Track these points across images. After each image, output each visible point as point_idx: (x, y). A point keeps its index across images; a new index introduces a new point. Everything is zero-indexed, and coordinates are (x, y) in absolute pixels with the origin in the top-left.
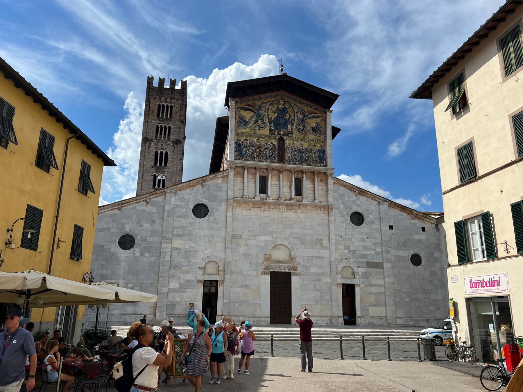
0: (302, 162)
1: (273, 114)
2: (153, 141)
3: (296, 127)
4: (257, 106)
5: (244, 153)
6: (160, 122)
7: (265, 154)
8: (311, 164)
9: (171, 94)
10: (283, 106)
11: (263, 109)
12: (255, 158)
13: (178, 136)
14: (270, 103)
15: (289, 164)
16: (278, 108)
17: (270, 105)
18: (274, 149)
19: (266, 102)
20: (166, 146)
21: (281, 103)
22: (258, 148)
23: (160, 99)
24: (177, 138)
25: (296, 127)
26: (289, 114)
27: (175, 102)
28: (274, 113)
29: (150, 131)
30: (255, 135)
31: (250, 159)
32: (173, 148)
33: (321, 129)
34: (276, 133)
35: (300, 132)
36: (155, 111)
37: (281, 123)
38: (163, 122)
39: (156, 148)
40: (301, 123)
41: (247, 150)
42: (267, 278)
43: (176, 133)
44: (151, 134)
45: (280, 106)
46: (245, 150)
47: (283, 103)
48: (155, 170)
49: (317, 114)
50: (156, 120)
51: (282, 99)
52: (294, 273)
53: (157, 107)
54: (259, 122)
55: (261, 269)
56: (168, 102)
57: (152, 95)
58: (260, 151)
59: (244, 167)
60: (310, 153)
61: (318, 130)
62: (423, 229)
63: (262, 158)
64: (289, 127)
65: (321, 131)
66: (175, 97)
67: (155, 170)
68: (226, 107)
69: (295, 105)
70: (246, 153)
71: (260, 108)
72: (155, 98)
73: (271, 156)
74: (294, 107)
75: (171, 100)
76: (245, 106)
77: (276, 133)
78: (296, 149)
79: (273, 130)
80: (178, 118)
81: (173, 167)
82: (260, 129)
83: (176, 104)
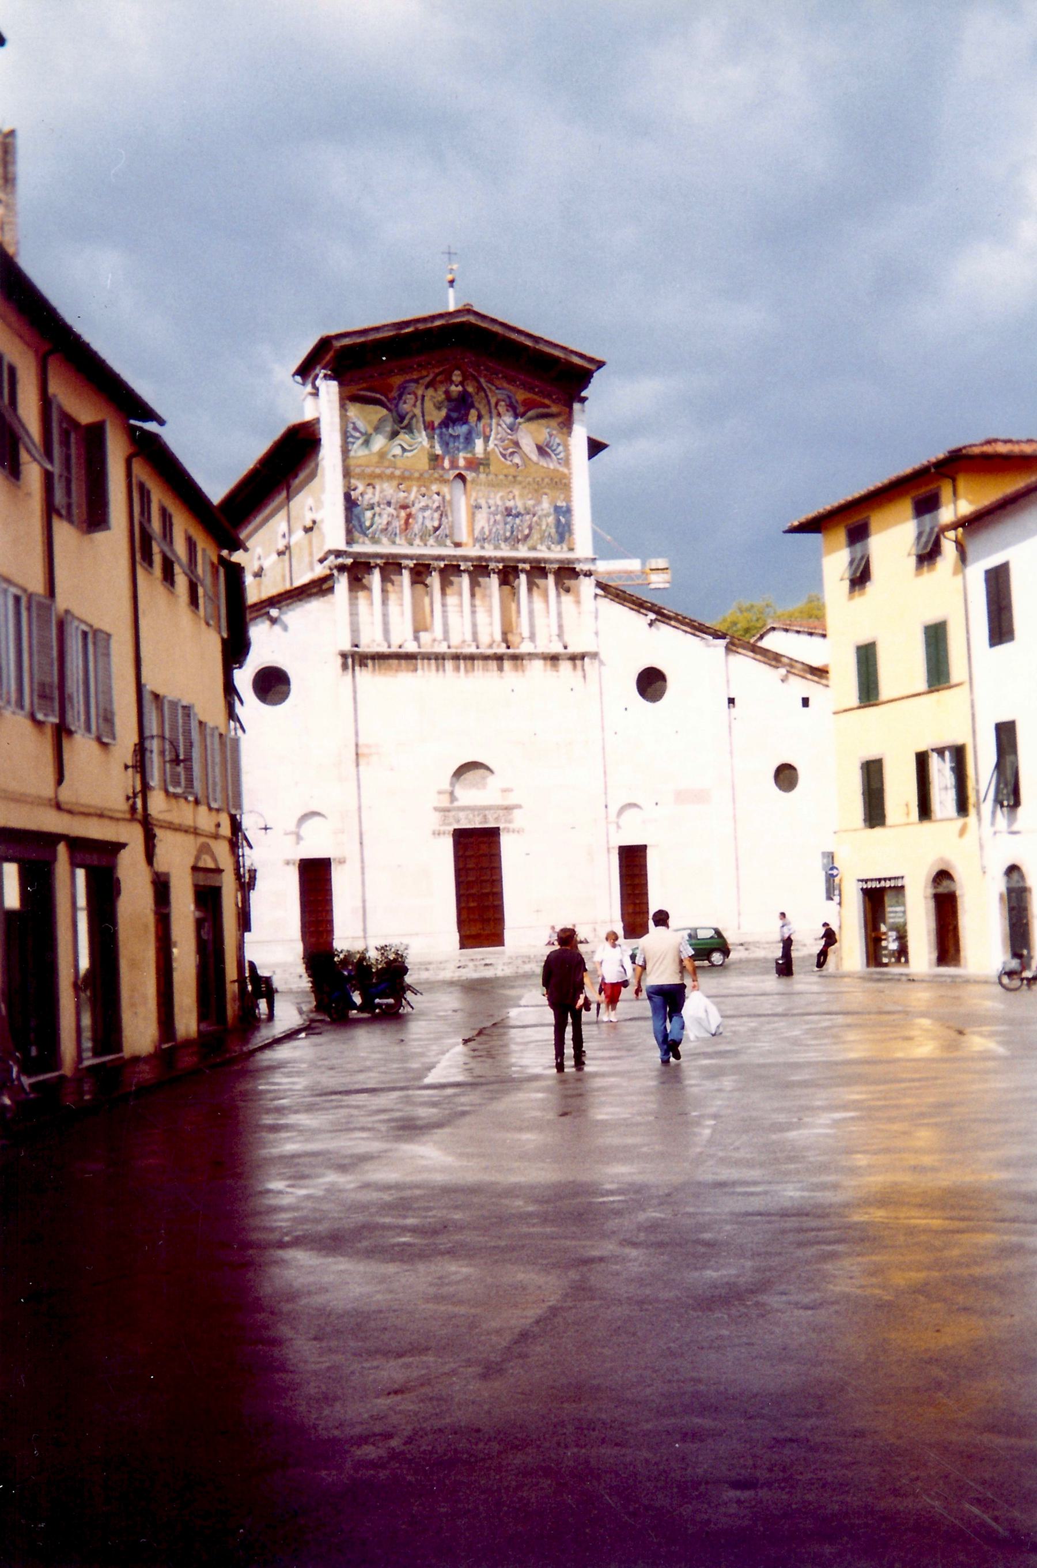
0: (514, 540)
1: (435, 412)
3: (496, 445)
4: (395, 390)
5: (368, 524)
7: (423, 523)
8: (539, 547)
10: (460, 388)
11: (410, 399)
12: (396, 534)
14: (427, 379)
15: (483, 548)
16: (447, 393)
17: (427, 387)
18: (444, 507)
19: (415, 377)
21: (454, 378)
22: (404, 507)
25: (496, 445)
26: (478, 410)
28: (439, 408)
30: (392, 473)
31: (385, 540)
33: (561, 448)
34: (447, 464)
35: (506, 459)
37: (458, 436)
40: (509, 434)
41: (374, 515)
42: (447, 845)
45: (453, 388)
46: (369, 514)
47: (460, 379)
49: (548, 407)
51: (458, 369)
52: (508, 830)
54: (402, 436)
55: (434, 820)
58: (409, 516)
59: (372, 565)
60: (534, 515)
61: (553, 451)
62: (806, 702)
63: (415, 535)
64: (479, 444)
65: (558, 454)
68: (298, 378)
69: (493, 384)
70: (371, 525)
71: (400, 396)
73: (436, 529)
74: (490, 389)
76: (362, 393)
77: (447, 464)
78: (498, 506)
79: (438, 456)
82: (406, 454)
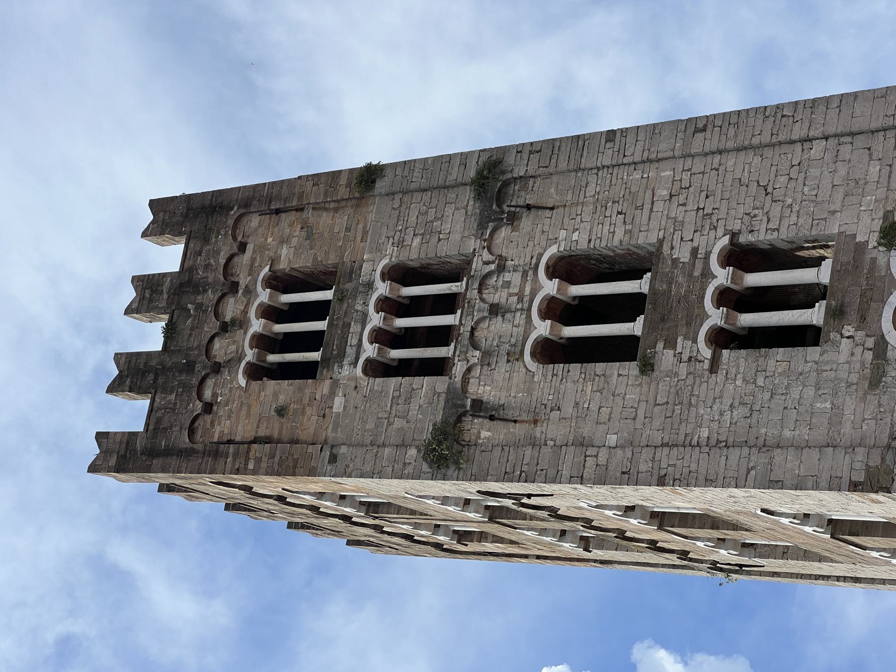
2: (465, 380)
6: (350, 352)
9: (205, 291)
13: (452, 195)
20: (507, 276)
23: (217, 368)
24: (467, 194)
27: (253, 260)
29: (398, 423)
32: (526, 222)
36: (282, 398)
38: (355, 328)
39: (514, 356)
43: (431, 217)
44: (414, 407)
48: (671, 344)
50: (335, 384)
53: (263, 389)
56: (245, 312)
57: (192, 432)
66: (222, 261)
67: (671, 344)
72: (208, 408)
75: (234, 287)
80: (342, 220)
81: (665, 193)
83: (261, 248)
